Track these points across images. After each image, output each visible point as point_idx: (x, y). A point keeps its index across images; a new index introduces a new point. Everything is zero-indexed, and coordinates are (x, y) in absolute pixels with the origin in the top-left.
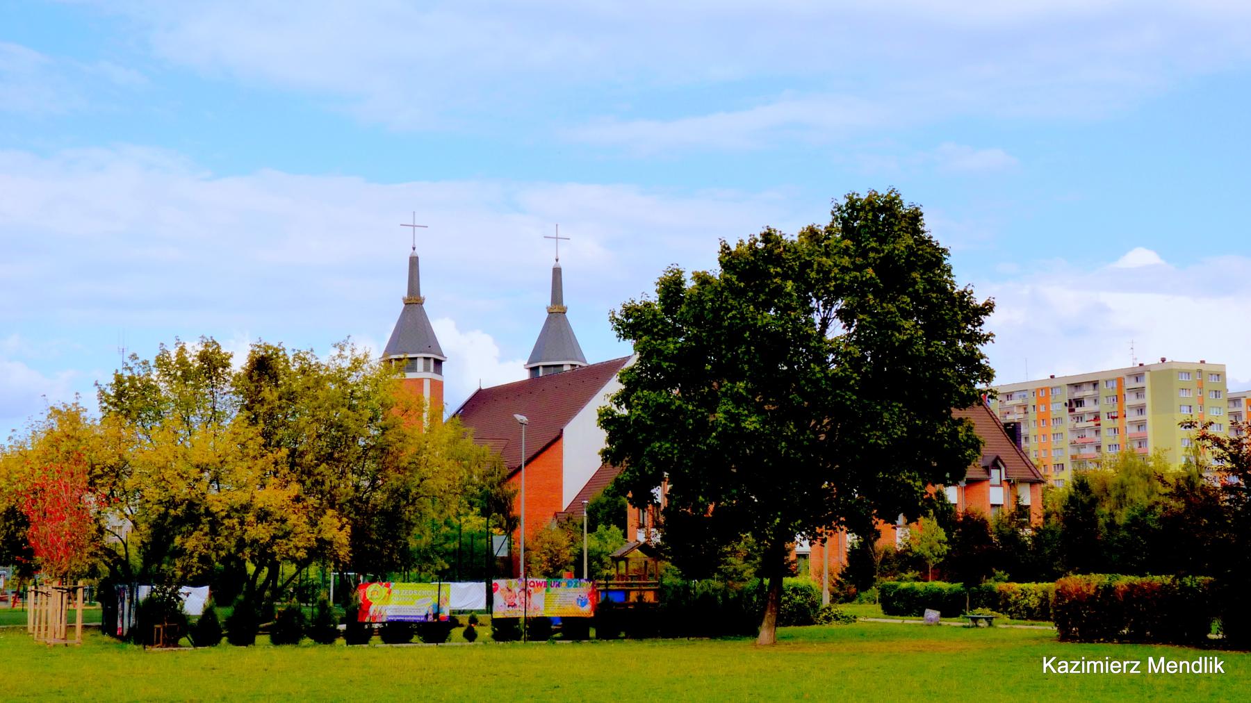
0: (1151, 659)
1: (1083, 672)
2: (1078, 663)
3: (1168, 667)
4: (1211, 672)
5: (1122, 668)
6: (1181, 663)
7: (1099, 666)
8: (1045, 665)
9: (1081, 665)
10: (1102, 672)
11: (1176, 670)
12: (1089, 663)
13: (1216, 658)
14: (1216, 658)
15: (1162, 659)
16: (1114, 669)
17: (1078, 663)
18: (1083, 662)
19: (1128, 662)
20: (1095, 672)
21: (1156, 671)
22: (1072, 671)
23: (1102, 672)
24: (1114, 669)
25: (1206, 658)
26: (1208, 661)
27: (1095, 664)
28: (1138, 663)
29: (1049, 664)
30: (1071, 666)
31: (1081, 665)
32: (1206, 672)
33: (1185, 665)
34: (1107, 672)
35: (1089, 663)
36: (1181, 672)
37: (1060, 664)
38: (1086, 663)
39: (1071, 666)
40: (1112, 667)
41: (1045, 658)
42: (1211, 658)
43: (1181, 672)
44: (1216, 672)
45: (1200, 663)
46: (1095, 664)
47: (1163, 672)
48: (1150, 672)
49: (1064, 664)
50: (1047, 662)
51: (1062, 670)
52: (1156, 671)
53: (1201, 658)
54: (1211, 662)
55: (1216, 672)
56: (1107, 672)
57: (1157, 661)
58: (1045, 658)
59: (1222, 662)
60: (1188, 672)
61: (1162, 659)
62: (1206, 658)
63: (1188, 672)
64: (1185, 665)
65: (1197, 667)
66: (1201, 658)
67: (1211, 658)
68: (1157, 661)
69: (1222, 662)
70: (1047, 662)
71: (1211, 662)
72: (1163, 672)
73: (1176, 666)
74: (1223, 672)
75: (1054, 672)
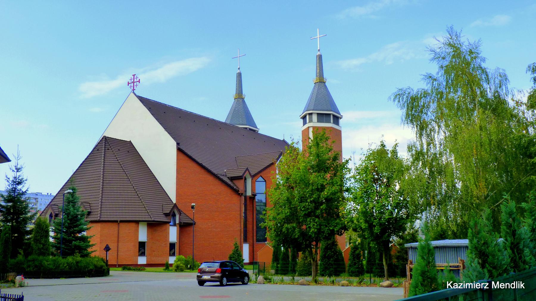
0: (493, 283)
1: (464, 288)
2: (462, 284)
3: (501, 286)
4: (519, 288)
5: (481, 286)
6: (506, 284)
7: (471, 286)
8: (448, 285)
9: (463, 285)
10: (472, 288)
11: (504, 287)
12: (466, 284)
13: (521, 282)
14: (521, 282)
15: (498, 283)
16: (478, 287)
17: (462, 284)
18: (464, 284)
19: (483, 284)
20: (469, 288)
21: (495, 287)
22: (459, 288)
23: (472, 288)
24: (478, 287)
25: (517, 282)
26: (518, 283)
27: (469, 284)
28: (488, 284)
29: (449, 284)
30: (459, 285)
31: (463, 285)
32: (517, 288)
33: (508, 285)
34: (474, 288)
35: (466, 284)
36: (506, 288)
37: (454, 284)
38: (465, 284)
39: (459, 285)
40: (476, 286)
41: (448, 282)
42: (519, 282)
43: (506, 288)
44: (521, 288)
45: (514, 284)
46: (469, 284)
47: (498, 288)
48: (493, 288)
49: (455, 285)
50: (449, 284)
51: (456, 287)
52: (495, 287)
53: (514, 282)
54: (519, 284)
55: (521, 288)
56: (474, 288)
57: (496, 283)
58: (448, 282)
59: (524, 284)
60: (509, 288)
61: (498, 283)
62: (517, 282)
63: (509, 288)
64: (508, 285)
65: (513, 286)
66: (514, 282)
67: (519, 282)
68: (496, 283)
69: (524, 284)
70: (449, 284)
71: (519, 284)
72: (498, 288)
73: (504, 285)
74: (524, 288)
75: (452, 288)
